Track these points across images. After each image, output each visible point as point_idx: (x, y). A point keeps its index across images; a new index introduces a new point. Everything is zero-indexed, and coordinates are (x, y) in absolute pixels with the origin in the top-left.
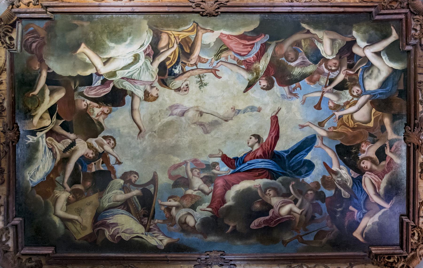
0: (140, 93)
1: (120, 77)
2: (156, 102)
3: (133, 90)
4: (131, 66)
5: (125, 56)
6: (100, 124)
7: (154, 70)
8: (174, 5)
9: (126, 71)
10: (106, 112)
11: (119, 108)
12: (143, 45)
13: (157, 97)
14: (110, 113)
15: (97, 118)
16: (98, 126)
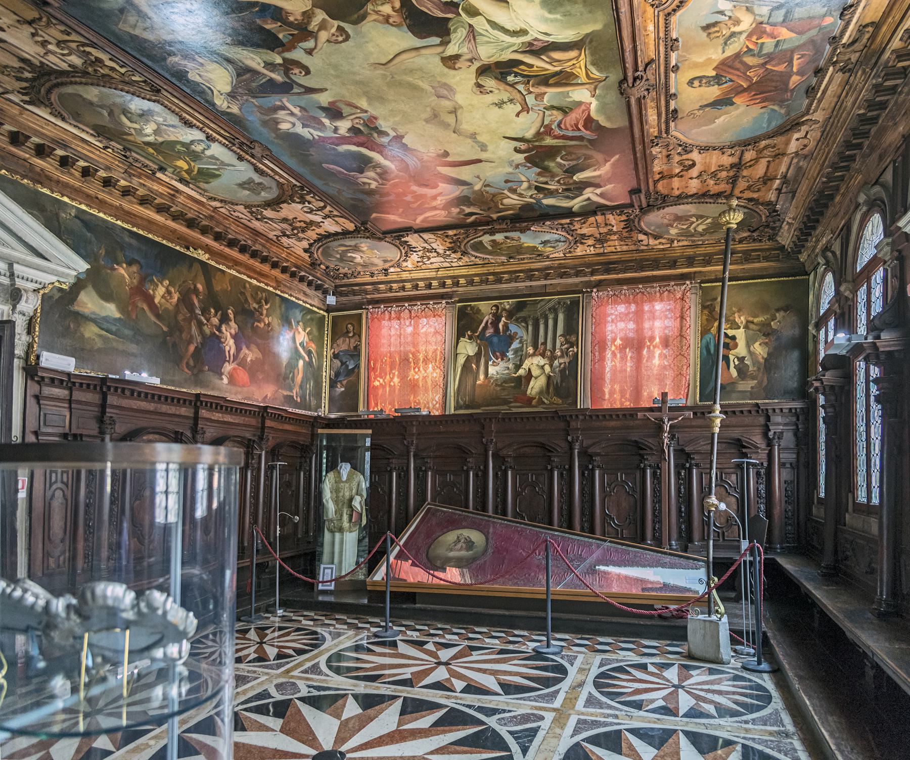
0: (452, 50)
1: (470, 22)
2: (446, 70)
3: (453, 42)
4: (499, 30)
5: (517, 19)
6: (363, 17)
7: (503, 56)
8: (639, 53)
9: (488, 27)
10: (391, 20)
11: (410, 33)
12: (550, 35)
13: (455, 69)
14: (392, 25)
15: (369, 11)
16: (356, 16)
